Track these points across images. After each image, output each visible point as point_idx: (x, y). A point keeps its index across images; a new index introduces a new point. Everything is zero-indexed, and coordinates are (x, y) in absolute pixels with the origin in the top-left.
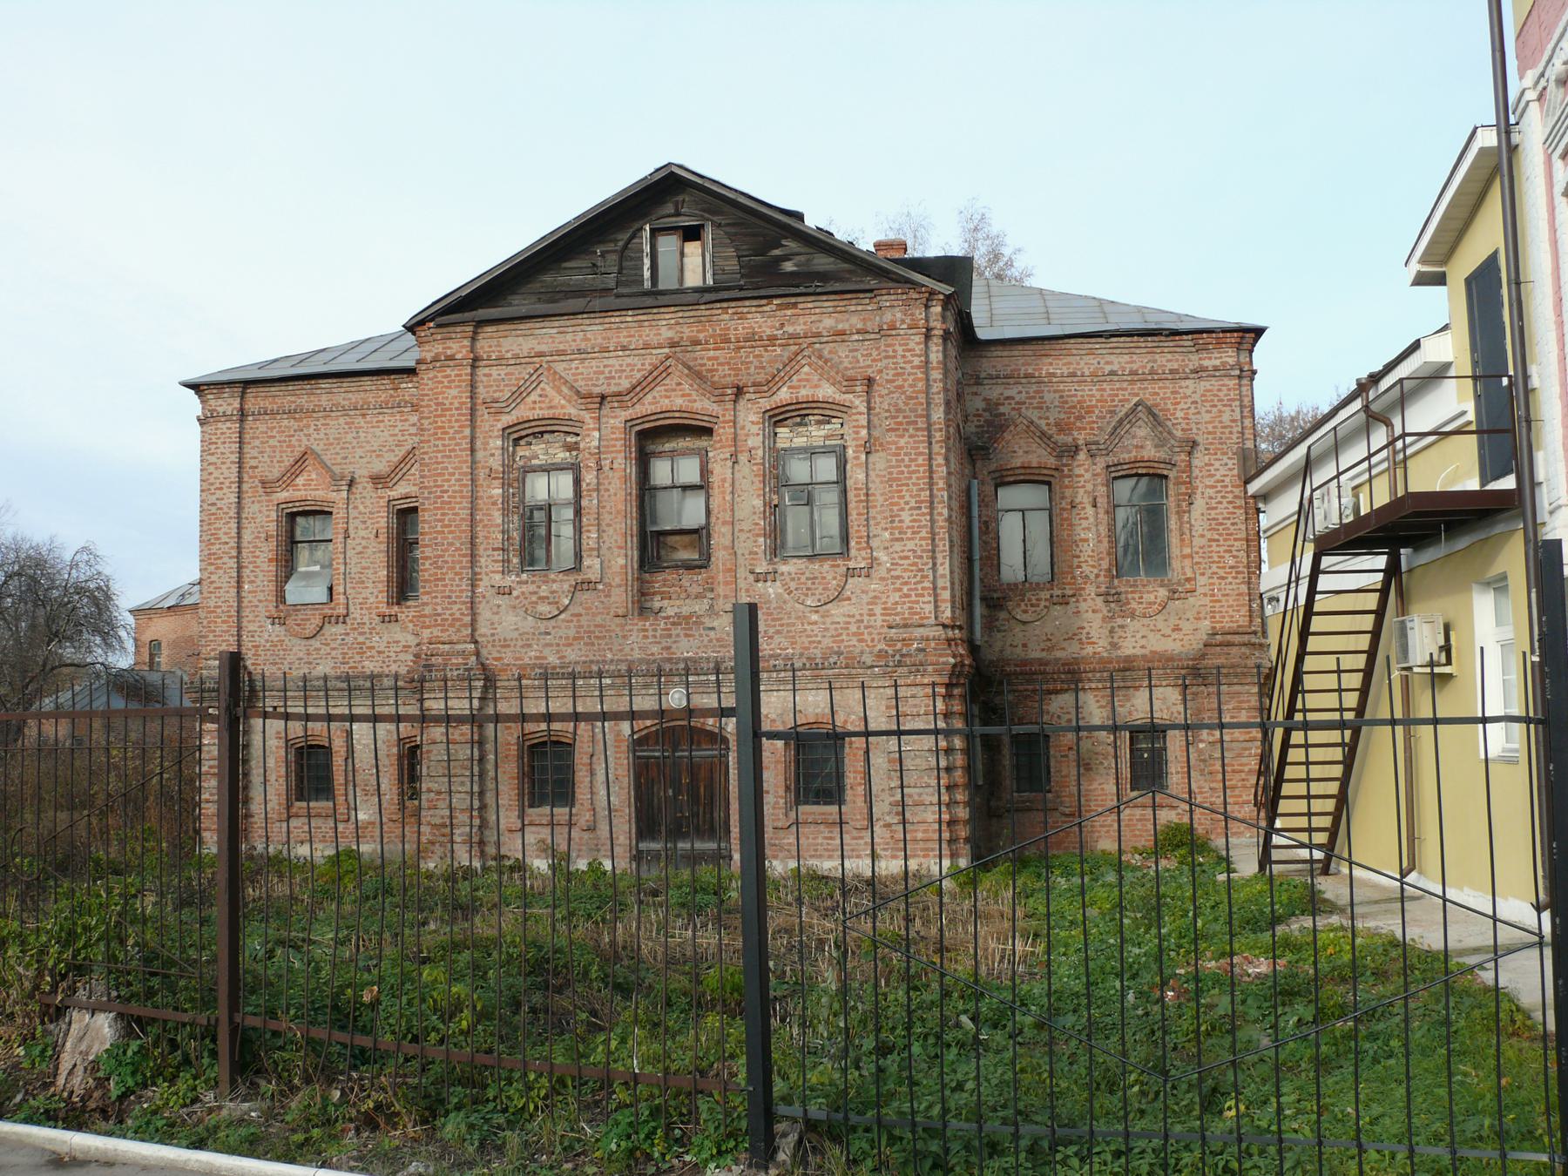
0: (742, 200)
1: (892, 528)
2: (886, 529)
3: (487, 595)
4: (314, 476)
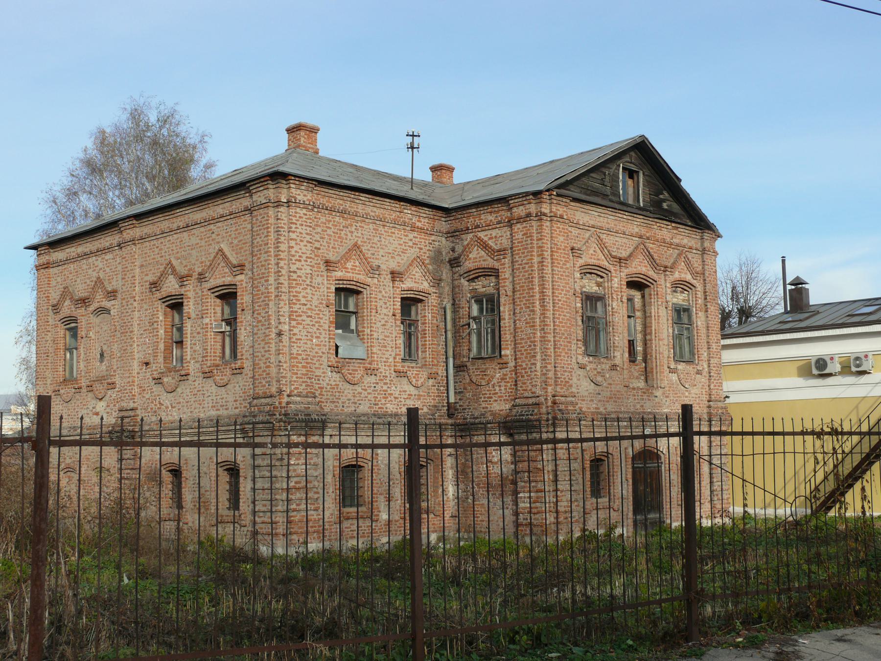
0: (665, 166)
4: (357, 264)
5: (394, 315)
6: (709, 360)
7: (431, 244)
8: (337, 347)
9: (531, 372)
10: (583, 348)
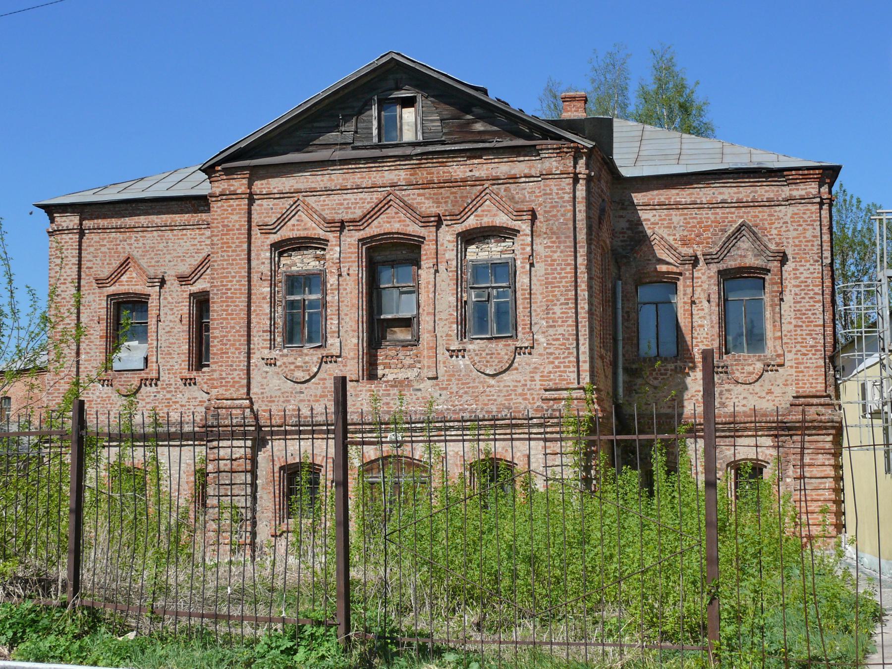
0: (443, 79)
1: (547, 318)
2: (544, 319)
3: (258, 364)
4: (134, 275)
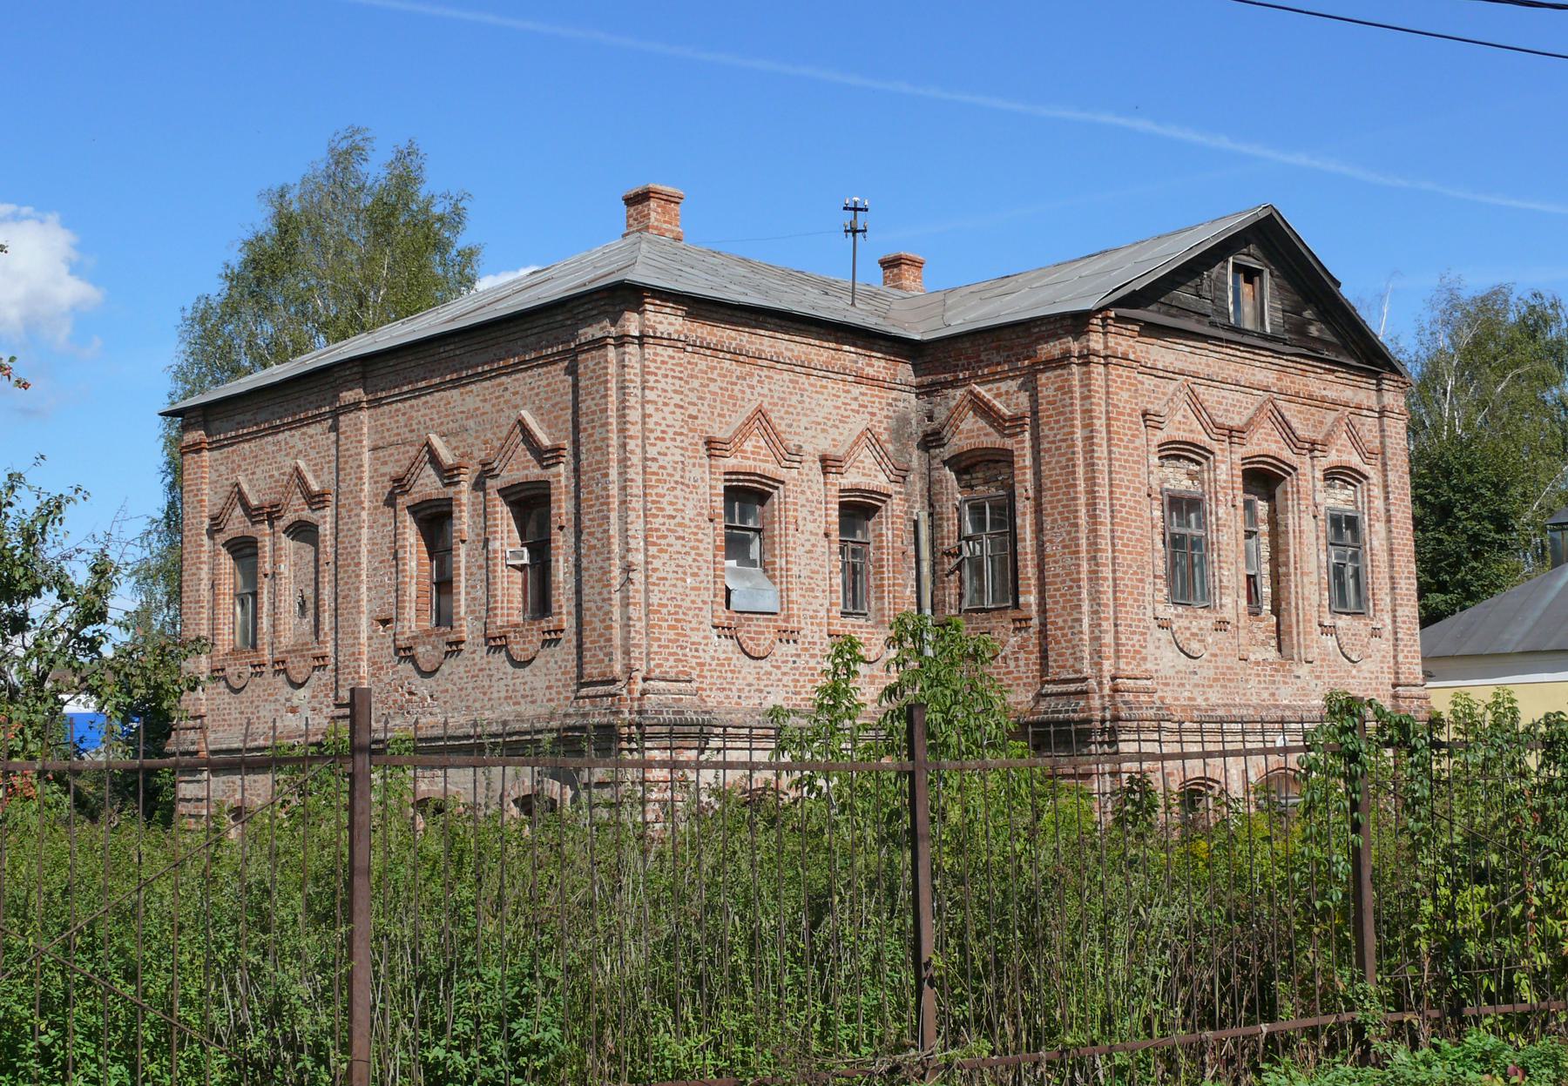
4: (763, 443)
5: (826, 535)
6: (1394, 611)
7: (891, 405)
8: (728, 592)
9: (1073, 634)
10: (1166, 591)
